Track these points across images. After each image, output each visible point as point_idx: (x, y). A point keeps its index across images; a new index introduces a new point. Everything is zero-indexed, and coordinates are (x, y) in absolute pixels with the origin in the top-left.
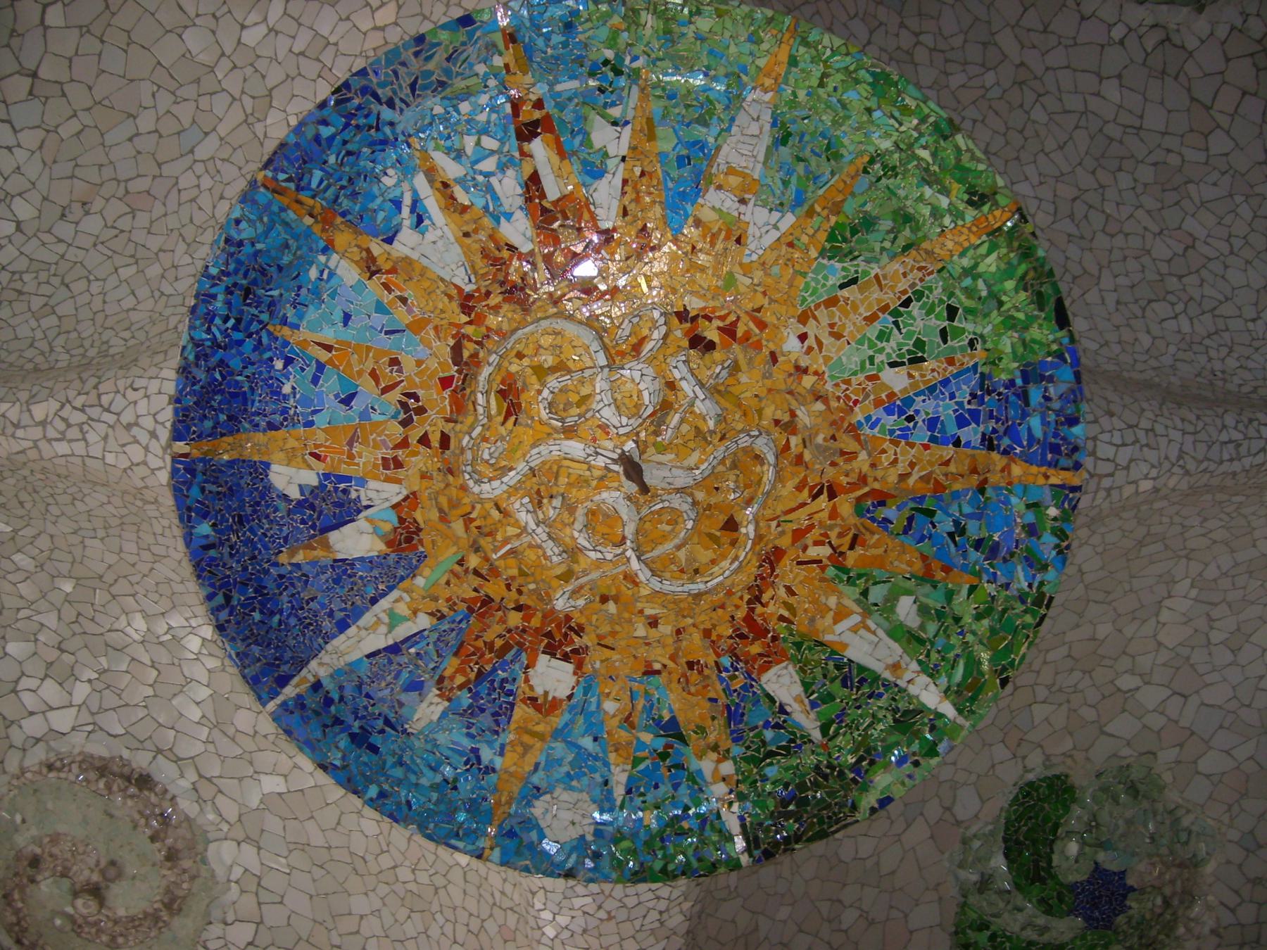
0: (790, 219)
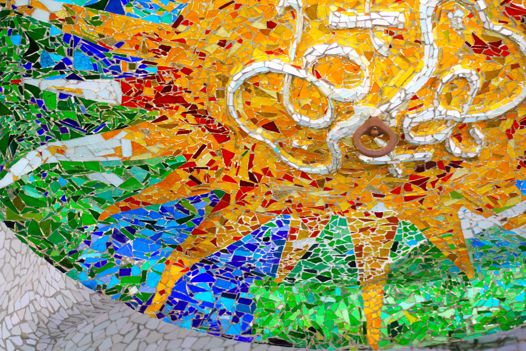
0: (468, 235)
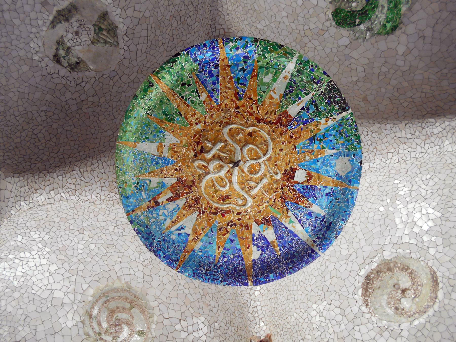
0: (166, 133)
